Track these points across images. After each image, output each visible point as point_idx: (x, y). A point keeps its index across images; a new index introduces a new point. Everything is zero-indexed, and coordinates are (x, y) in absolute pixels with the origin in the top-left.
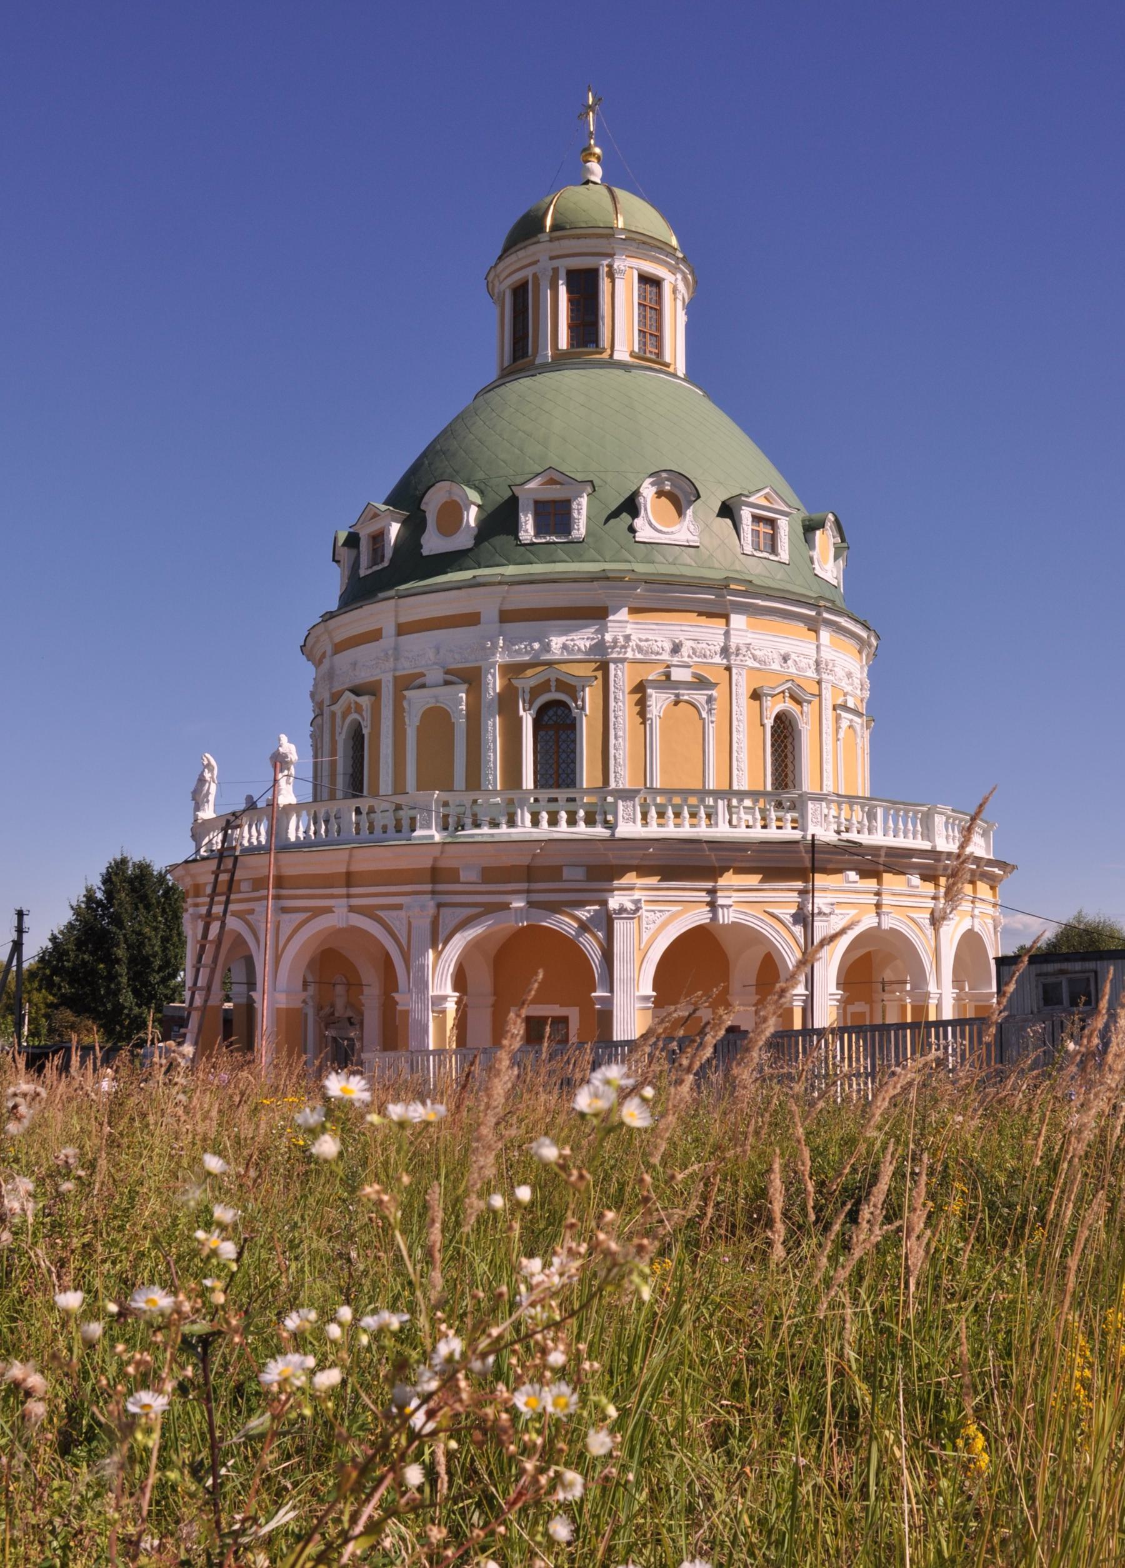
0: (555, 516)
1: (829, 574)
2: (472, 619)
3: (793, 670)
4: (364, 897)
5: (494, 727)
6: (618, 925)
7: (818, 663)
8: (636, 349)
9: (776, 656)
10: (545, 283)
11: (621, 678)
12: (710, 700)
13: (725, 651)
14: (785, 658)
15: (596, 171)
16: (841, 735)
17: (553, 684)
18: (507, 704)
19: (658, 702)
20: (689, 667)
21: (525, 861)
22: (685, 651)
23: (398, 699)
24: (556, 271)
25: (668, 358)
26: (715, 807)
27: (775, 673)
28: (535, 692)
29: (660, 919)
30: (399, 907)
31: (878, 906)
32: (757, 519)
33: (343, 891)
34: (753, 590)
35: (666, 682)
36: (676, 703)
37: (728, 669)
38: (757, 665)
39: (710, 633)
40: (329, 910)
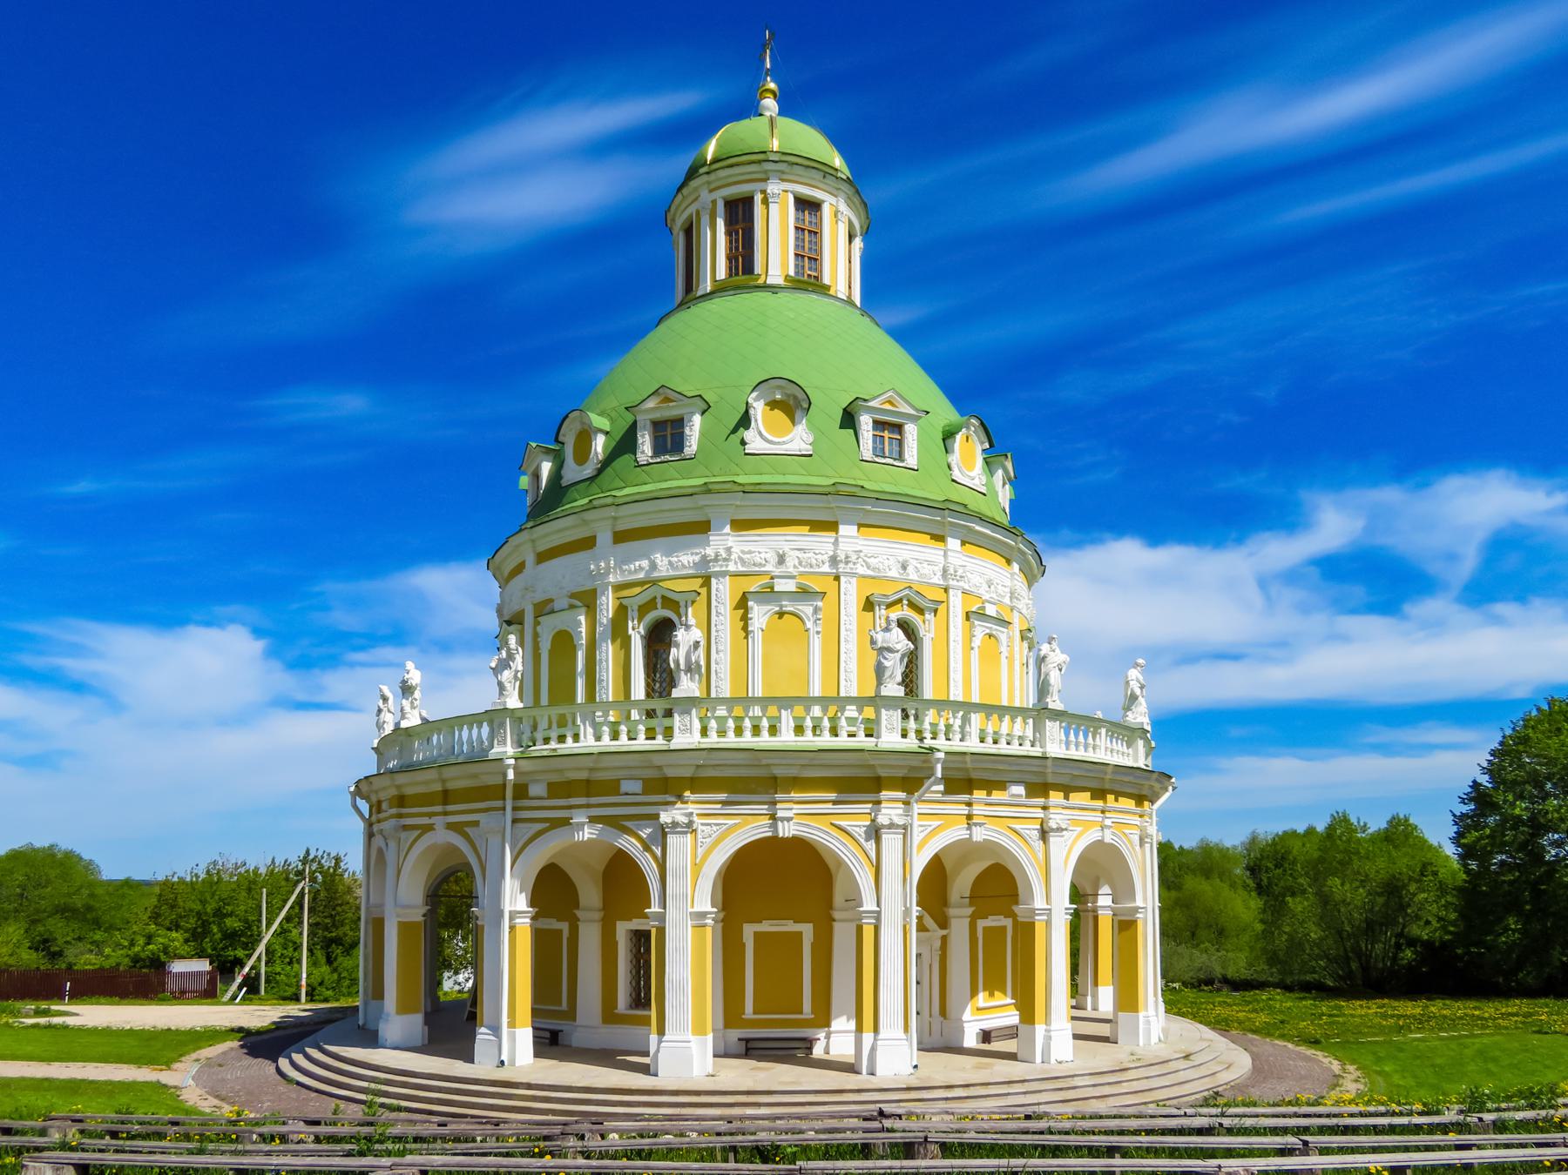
0: (670, 436)
1: (977, 481)
2: (588, 543)
3: (913, 576)
4: (460, 813)
6: (672, 840)
7: (945, 571)
8: (792, 273)
9: (892, 561)
10: (705, 219)
11: (724, 592)
13: (834, 560)
14: (904, 567)
16: (977, 642)
17: (659, 601)
19: (760, 615)
20: (793, 577)
21: (584, 775)
22: (791, 562)
24: (714, 202)
25: (826, 280)
26: (779, 719)
27: (893, 580)
28: (643, 610)
30: (476, 824)
31: (969, 817)
32: (879, 425)
33: (439, 809)
35: (768, 594)
36: (781, 614)
37: (837, 578)
38: (870, 573)
39: (822, 544)
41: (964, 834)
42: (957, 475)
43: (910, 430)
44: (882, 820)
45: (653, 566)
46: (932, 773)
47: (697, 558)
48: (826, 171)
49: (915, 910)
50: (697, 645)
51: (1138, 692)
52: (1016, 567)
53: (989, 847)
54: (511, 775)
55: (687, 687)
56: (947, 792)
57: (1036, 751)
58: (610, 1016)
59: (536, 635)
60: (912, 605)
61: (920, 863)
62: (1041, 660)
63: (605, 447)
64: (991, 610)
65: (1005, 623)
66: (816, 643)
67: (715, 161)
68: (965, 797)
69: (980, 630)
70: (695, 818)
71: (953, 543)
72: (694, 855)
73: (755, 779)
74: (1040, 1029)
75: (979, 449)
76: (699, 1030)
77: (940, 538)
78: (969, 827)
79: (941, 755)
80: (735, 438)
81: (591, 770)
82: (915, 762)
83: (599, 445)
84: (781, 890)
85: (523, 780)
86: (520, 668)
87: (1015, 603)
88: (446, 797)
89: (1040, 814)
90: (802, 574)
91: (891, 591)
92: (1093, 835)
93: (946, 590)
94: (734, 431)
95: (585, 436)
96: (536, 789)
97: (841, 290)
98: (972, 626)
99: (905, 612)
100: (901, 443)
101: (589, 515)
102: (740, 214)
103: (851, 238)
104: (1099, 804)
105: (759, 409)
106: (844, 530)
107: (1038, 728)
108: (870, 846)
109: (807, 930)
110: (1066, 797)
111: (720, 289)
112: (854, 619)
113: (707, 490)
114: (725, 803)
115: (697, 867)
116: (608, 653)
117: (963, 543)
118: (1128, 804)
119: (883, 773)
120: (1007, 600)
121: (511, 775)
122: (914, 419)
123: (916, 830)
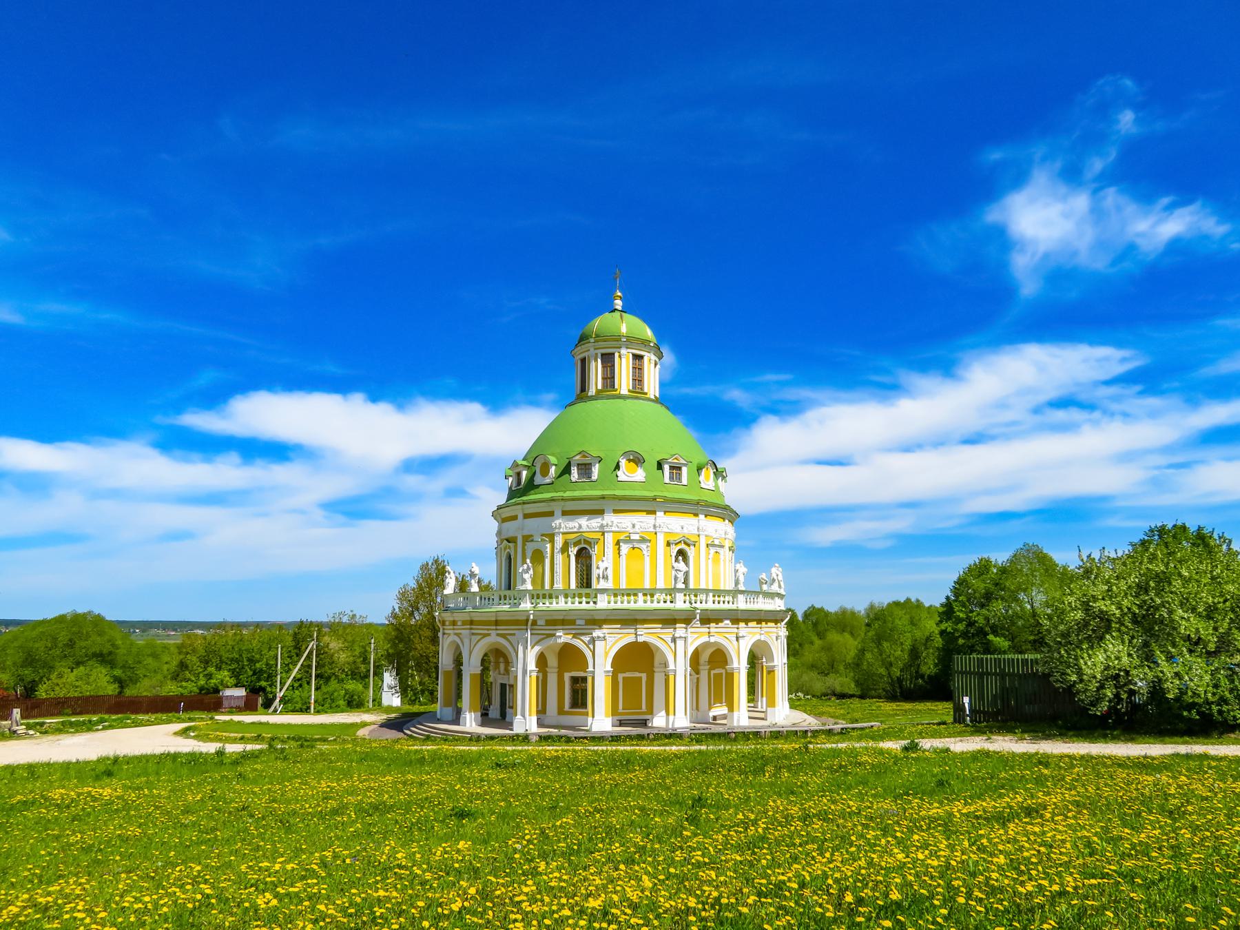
0: (585, 469)
2: (551, 514)
3: (685, 531)
4: (503, 630)
5: (559, 558)
11: (610, 539)
15: (619, 304)
18: (565, 549)
19: (625, 548)
23: (524, 545)
29: (613, 640)
32: (672, 468)
34: (668, 501)
35: (628, 540)
40: (489, 635)
42: (703, 485)
43: (684, 469)
45: (580, 526)
57: (734, 607)
58: (561, 711)
61: (691, 650)
62: (736, 571)
64: (717, 542)
65: (722, 547)
66: (647, 560)
69: (712, 550)
72: (603, 649)
73: (630, 620)
74: (736, 714)
76: (607, 716)
77: (696, 515)
84: (638, 662)
88: (497, 623)
91: (677, 538)
92: (757, 637)
99: (682, 546)
100: (680, 475)
102: (608, 359)
105: (623, 462)
106: (658, 514)
108: (672, 645)
109: (644, 676)
113: (603, 497)
115: (607, 653)
123: (689, 641)
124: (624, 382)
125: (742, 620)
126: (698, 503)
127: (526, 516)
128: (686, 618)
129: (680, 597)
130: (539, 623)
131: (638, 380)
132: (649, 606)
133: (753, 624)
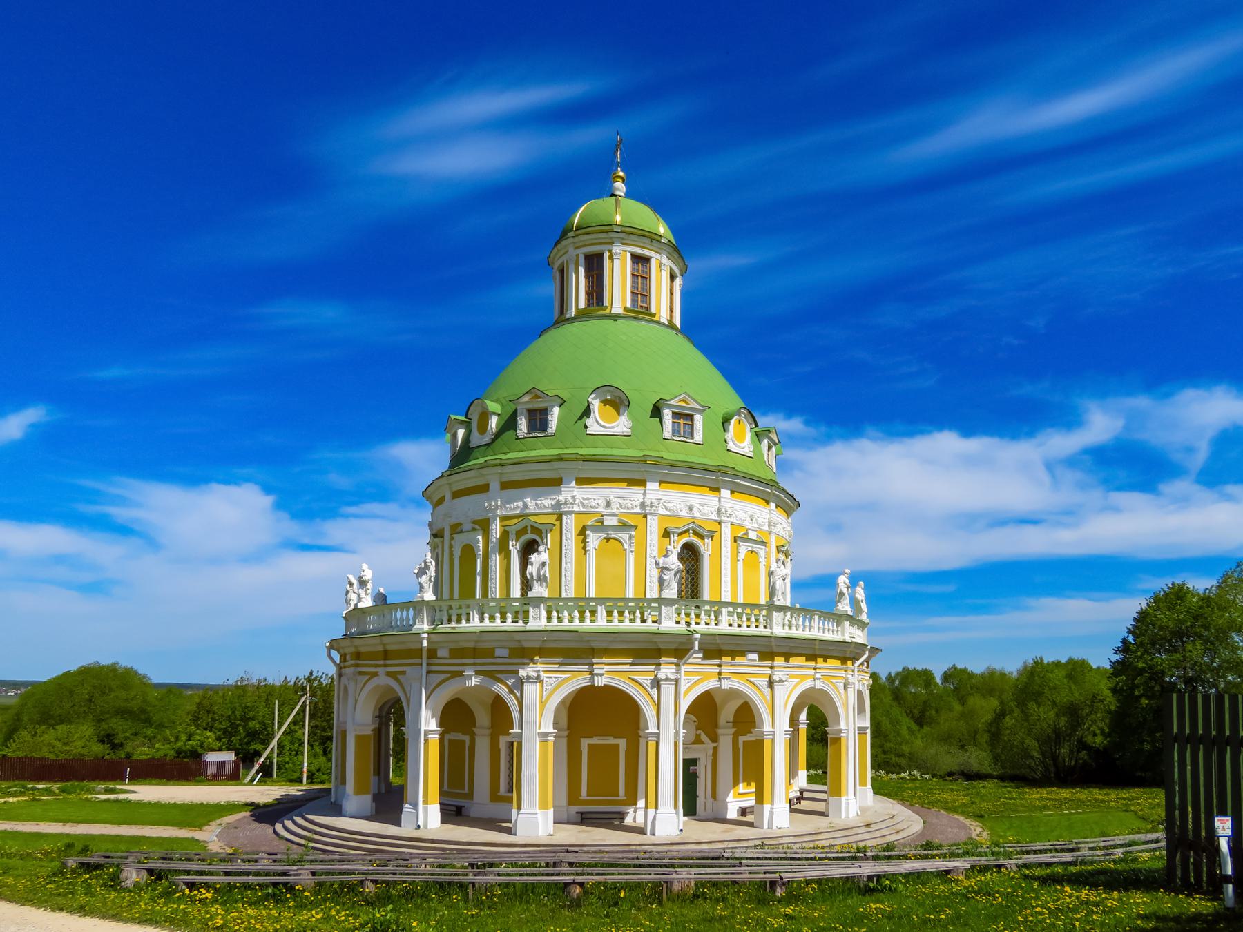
0: (538, 420)
2: (484, 488)
3: (697, 515)
6: (527, 687)
7: (719, 511)
8: (629, 305)
9: (682, 505)
10: (572, 267)
12: (631, 537)
13: (643, 505)
14: (691, 509)
15: (620, 188)
19: (594, 540)
21: (471, 645)
24: (578, 256)
25: (653, 310)
27: (683, 517)
28: (519, 534)
30: (404, 673)
32: (676, 415)
33: (381, 662)
34: (661, 464)
35: (600, 527)
36: (608, 539)
37: (645, 516)
39: (635, 494)
40: (375, 674)
41: (717, 684)
42: (731, 446)
43: (698, 419)
44: (661, 676)
45: (526, 506)
46: (693, 644)
47: (554, 502)
48: (653, 238)
49: (682, 731)
50: (544, 564)
51: (845, 590)
52: (773, 505)
53: (734, 693)
54: (425, 644)
55: (538, 590)
56: (704, 658)
57: (767, 632)
59: (451, 547)
60: (696, 533)
61: (685, 704)
63: (497, 424)
64: (752, 535)
66: (631, 558)
67: (579, 228)
68: (717, 661)
69: (744, 548)
70: (542, 674)
71: (725, 493)
72: (541, 698)
73: (579, 649)
75: (748, 427)
77: (716, 490)
78: (720, 680)
79: (698, 636)
80: (580, 423)
81: (477, 641)
82: (682, 640)
83: (494, 422)
84: (601, 721)
85: (434, 646)
86: (433, 574)
87: (772, 529)
89: (769, 671)
90: (622, 513)
92: (808, 684)
93: (720, 523)
94: (580, 418)
95: (485, 416)
96: (443, 653)
97: (664, 317)
98: (738, 546)
100: (692, 426)
101: (485, 471)
102: (594, 265)
103: (672, 278)
104: (812, 664)
105: (596, 405)
106: (650, 485)
107: (769, 617)
108: (654, 692)
110: (787, 660)
111: (581, 315)
112: (656, 542)
113: (560, 458)
114: (560, 664)
115: (543, 704)
116: (496, 560)
117: (732, 492)
118: (837, 663)
119: (662, 646)
120: (766, 528)
121: (425, 644)
122: (700, 411)
123: (683, 682)
124: (619, 295)
125: (780, 654)
126: (718, 471)
127: (457, 495)
128: (679, 648)
129: (668, 613)
130: (441, 653)
131: (641, 293)
132: (616, 625)
133: (801, 661)
